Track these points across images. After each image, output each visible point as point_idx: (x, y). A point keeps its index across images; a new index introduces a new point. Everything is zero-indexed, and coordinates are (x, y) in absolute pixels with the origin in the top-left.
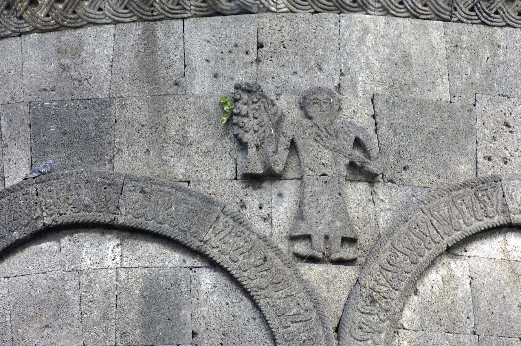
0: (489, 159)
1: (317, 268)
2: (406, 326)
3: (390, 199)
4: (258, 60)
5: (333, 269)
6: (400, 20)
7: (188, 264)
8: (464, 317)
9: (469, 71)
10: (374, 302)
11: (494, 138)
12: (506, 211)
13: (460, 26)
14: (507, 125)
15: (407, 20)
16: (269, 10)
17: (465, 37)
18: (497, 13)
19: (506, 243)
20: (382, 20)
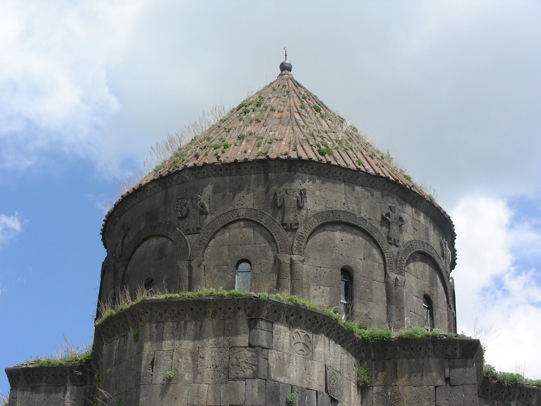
0: (238, 205)
1: (190, 236)
2: (210, 246)
3: (211, 218)
4: (185, 193)
5: (194, 235)
6: (218, 177)
7: (167, 240)
8: (226, 242)
9: (235, 186)
10: (201, 241)
11: (240, 200)
12: (238, 216)
13: (234, 176)
14: (243, 197)
15: (220, 177)
16: (189, 181)
17: (234, 179)
18: (242, 172)
19: (239, 223)
20: (214, 178)
